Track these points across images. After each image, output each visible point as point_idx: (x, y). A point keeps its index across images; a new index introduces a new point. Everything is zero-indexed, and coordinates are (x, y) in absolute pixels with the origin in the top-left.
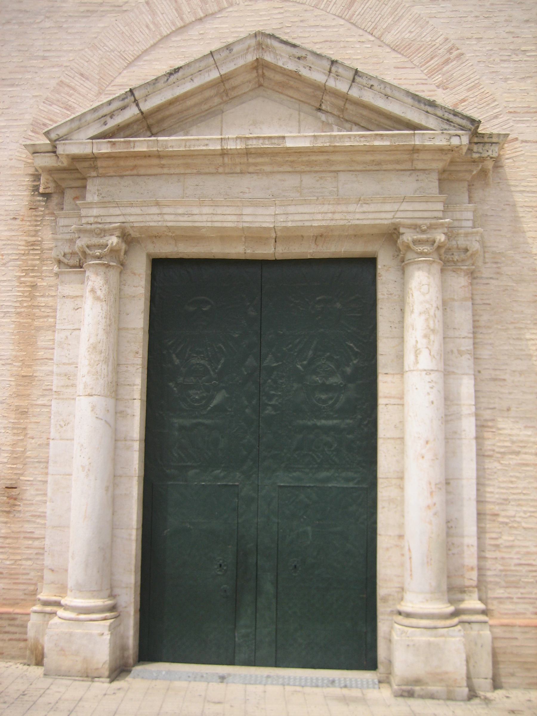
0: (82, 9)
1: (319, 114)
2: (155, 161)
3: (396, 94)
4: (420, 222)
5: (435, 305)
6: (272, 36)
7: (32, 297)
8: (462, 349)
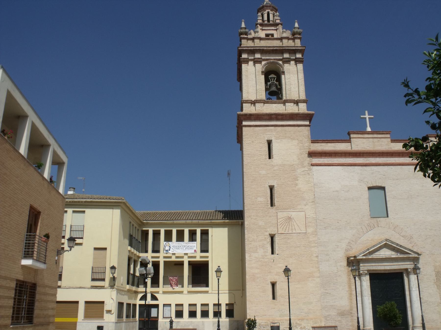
3: (407, 249)
4: (411, 268)
7: (350, 280)
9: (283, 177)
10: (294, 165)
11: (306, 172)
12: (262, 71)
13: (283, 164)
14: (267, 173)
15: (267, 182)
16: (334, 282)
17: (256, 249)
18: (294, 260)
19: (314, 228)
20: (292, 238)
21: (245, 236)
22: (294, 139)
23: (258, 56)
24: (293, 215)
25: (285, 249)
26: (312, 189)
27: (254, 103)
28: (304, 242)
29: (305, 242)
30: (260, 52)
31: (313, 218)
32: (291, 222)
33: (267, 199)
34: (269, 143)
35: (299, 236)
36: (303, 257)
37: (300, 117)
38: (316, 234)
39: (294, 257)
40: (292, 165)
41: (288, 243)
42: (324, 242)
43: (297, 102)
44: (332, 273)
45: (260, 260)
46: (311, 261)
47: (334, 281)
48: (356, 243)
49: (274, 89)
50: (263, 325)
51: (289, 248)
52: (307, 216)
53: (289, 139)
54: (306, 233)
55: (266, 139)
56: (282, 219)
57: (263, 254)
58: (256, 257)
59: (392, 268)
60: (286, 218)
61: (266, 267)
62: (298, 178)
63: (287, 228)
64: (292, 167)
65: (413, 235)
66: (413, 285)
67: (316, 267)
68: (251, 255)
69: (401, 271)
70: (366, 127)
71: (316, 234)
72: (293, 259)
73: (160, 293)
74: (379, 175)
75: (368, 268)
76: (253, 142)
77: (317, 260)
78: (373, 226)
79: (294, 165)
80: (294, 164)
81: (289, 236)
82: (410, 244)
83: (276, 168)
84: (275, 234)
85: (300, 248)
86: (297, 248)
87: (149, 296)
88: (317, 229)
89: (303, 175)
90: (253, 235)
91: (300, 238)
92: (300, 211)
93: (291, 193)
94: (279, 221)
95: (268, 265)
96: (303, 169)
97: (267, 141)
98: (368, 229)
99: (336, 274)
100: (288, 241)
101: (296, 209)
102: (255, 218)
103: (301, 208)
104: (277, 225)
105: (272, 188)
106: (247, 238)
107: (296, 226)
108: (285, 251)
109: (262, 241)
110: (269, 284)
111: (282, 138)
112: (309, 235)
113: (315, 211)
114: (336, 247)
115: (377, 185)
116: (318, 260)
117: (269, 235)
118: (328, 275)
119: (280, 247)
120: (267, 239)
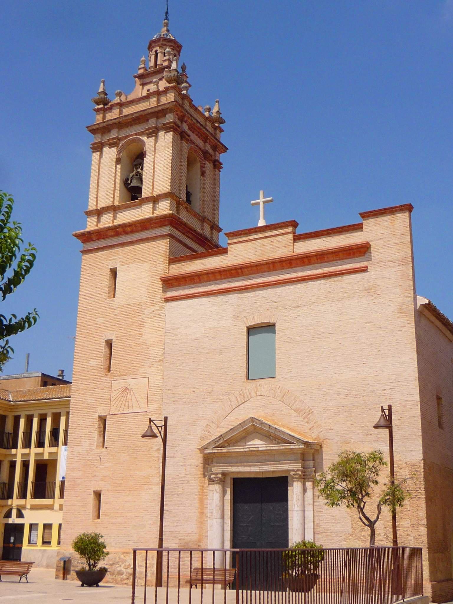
0: (212, 401)
1: (270, 437)
2: (229, 453)
4: (294, 469)
5: (299, 492)
6: (255, 418)
7: (203, 490)
8: (310, 503)
9: (125, 324)
10: (142, 304)
11: (156, 312)
12: (116, 159)
13: (127, 305)
14: (105, 321)
15: (104, 336)
16: (179, 493)
17: (81, 440)
18: (126, 456)
19: (158, 404)
20: (127, 420)
21: (70, 421)
22: (145, 262)
23: (114, 134)
24: (132, 383)
25: (117, 439)
26: (161, 340)
27: (99, 213)
28: (143, 427)
29: (144, 426)
30: (116, 128)
31: (159, 386)
32: (128, 395)
33: (102, 361)
34: (114, 272)
35: (137, 416)
36: (138, 450)
37: (156, 223)
38: (160, 413)
39: (128, 451)
40: (139, 304)
41: (121, 429)
42: (171, 425)
43: (155, 200)
44: (177, 477)
45: (84, 457)
46: (150, 457)
47: (179, 491)
48: (218, 427)
49: (134, 183)
50: (77, 559)
51: (122, 437)
52: (151, 384)
53: (139, 262)
54: (147, 412)
55: (110, 267)
56: (117, 392)
57: (88, 448)
58: (79, 453)
59: (263, 468)
60: (122, 389)
61: (90, 468)
62: (145, 324)
63: (123, 406)
64: (139, 306)
65: (313, 406)
66: (296, 501)
67: (155, 467)
68: (73, 449)
69: (284, 475)
70: (259, 219)
71: (160, 412)
72: (126, 455)
73: (55, 508)
74: (268, 302)
75: (224, 470)
76: (92, 275)
77: (157, 455)
78: (248, 395)
79: (142, 304)
80: (141, 302)
81: (124, 418)
82: (307, 424)
83: (117, 312)
84: (106, 416)
85: (136, 437)
86: (132, 437)
87: (14, 512)
88: (162, 405)
89: (151, 318)
90: (79, 419)
91: (138, 420)
92: (142, 377)
93: (133, 349)
94: (112, 395)
95: (93, 464)
96: (153, 308)
97: (111, 269)
98: (239, 400)
99: (184, 479)
100: (122, 425)
101: (137, 374)
102: (83, 392)
103: (144, 372)
104: (110, 402)
105: (109, 344)
106: (72, 423)
107: (134, 400)
108: (116, 442)
109: (88, 427)
110: (91, 495)
111: (129, 263)
112: (150, 414)
113: (162, 375)
114: (187, 433)
115: (263, 322)
116: (158, 456)
117: (97, 417)
118: (171, 481)
119: (111, 436)
120: (95, 425)
